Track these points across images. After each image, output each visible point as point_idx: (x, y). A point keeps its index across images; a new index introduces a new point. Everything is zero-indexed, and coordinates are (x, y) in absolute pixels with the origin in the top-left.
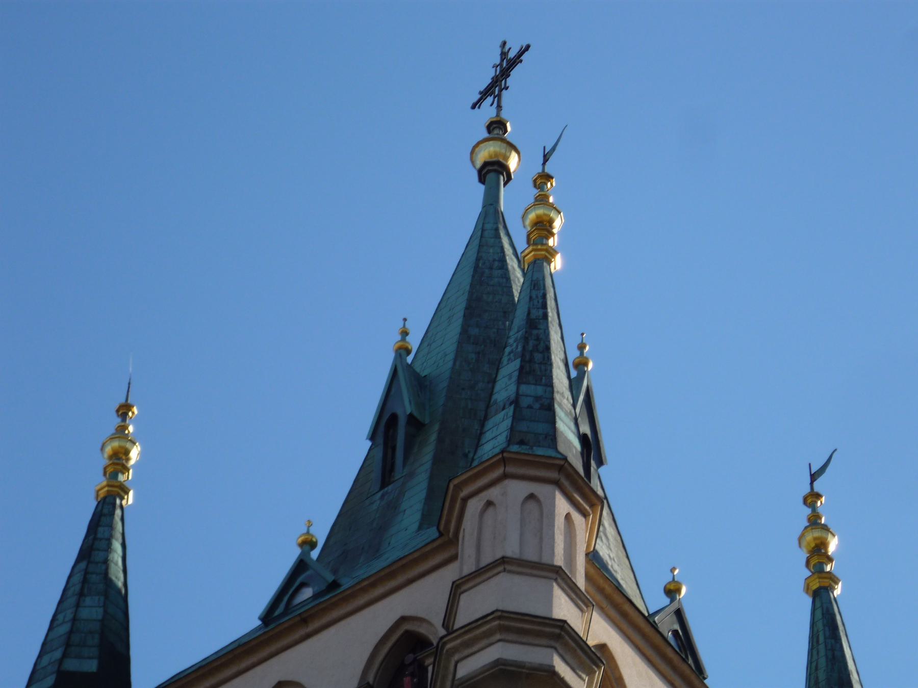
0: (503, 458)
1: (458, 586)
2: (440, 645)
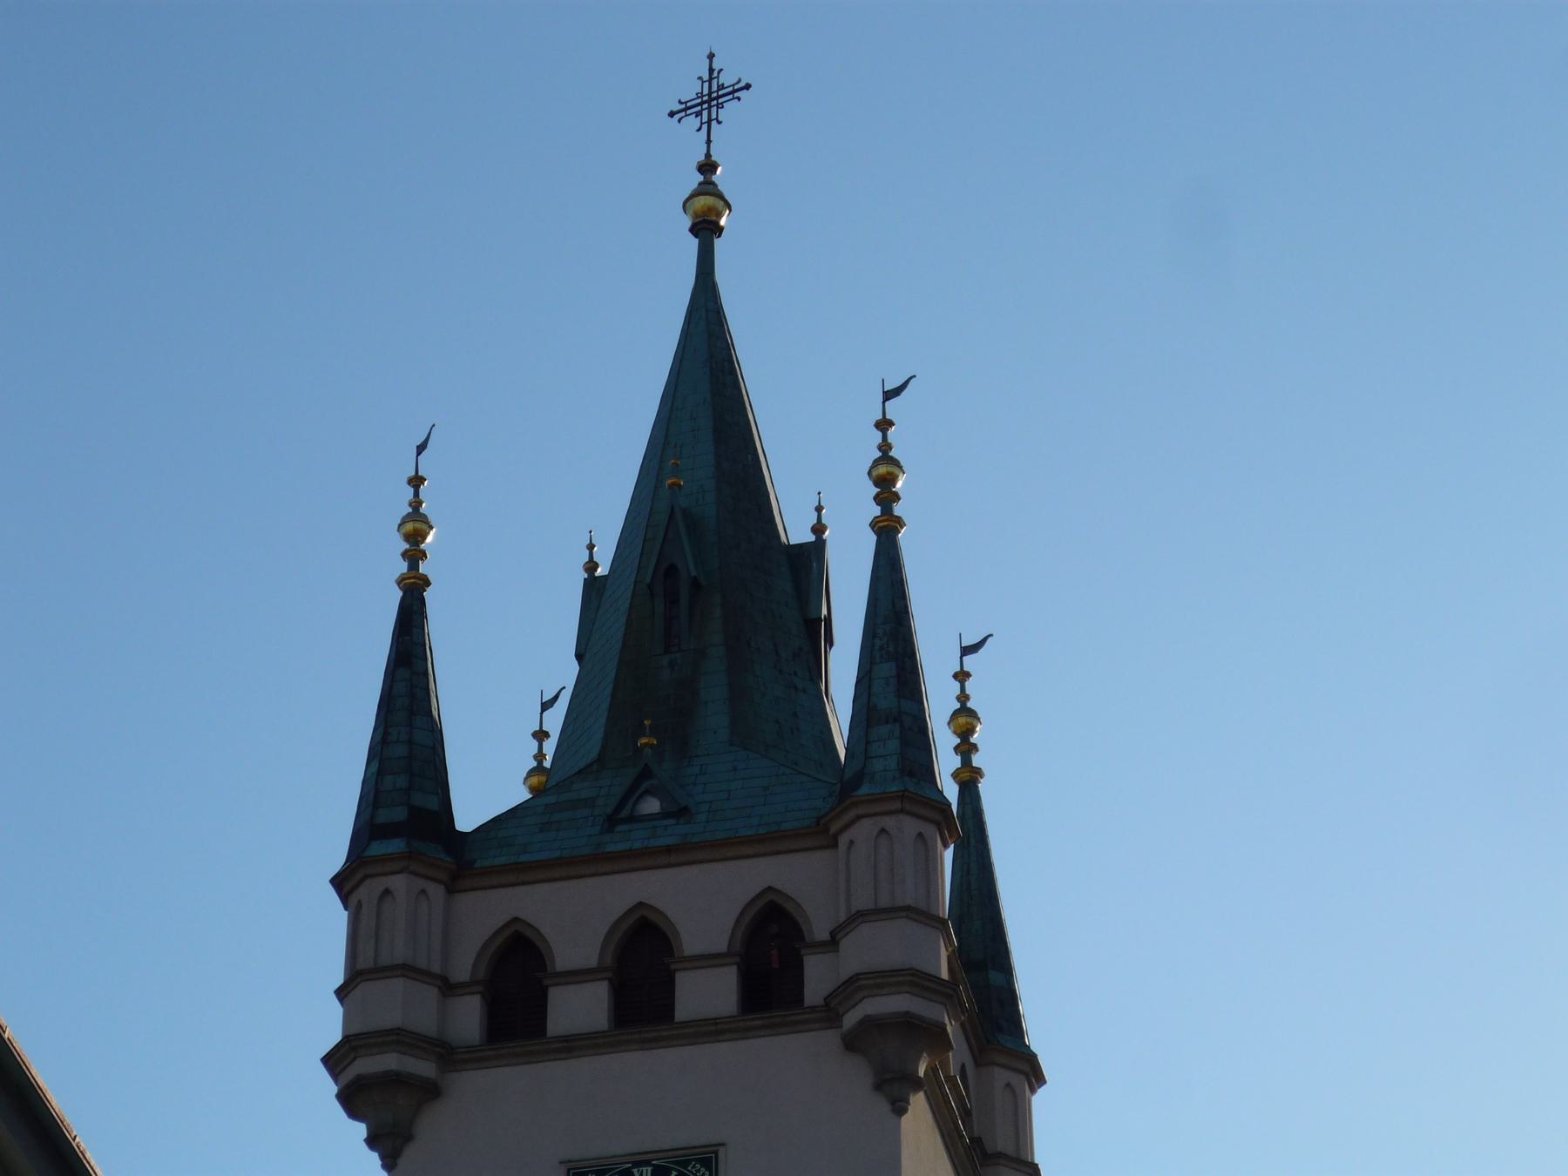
0: (903, 796)
1: (861, 915)
2: (854, 978)
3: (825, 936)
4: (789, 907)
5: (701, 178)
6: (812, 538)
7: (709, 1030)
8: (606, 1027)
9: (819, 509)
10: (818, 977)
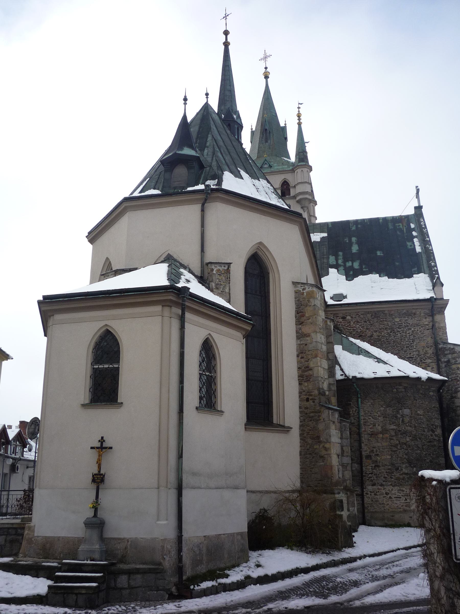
3: (294, 186)
4: (288, 181)
5: (265, 70)
9: (285, 121)
10: (293, 192)
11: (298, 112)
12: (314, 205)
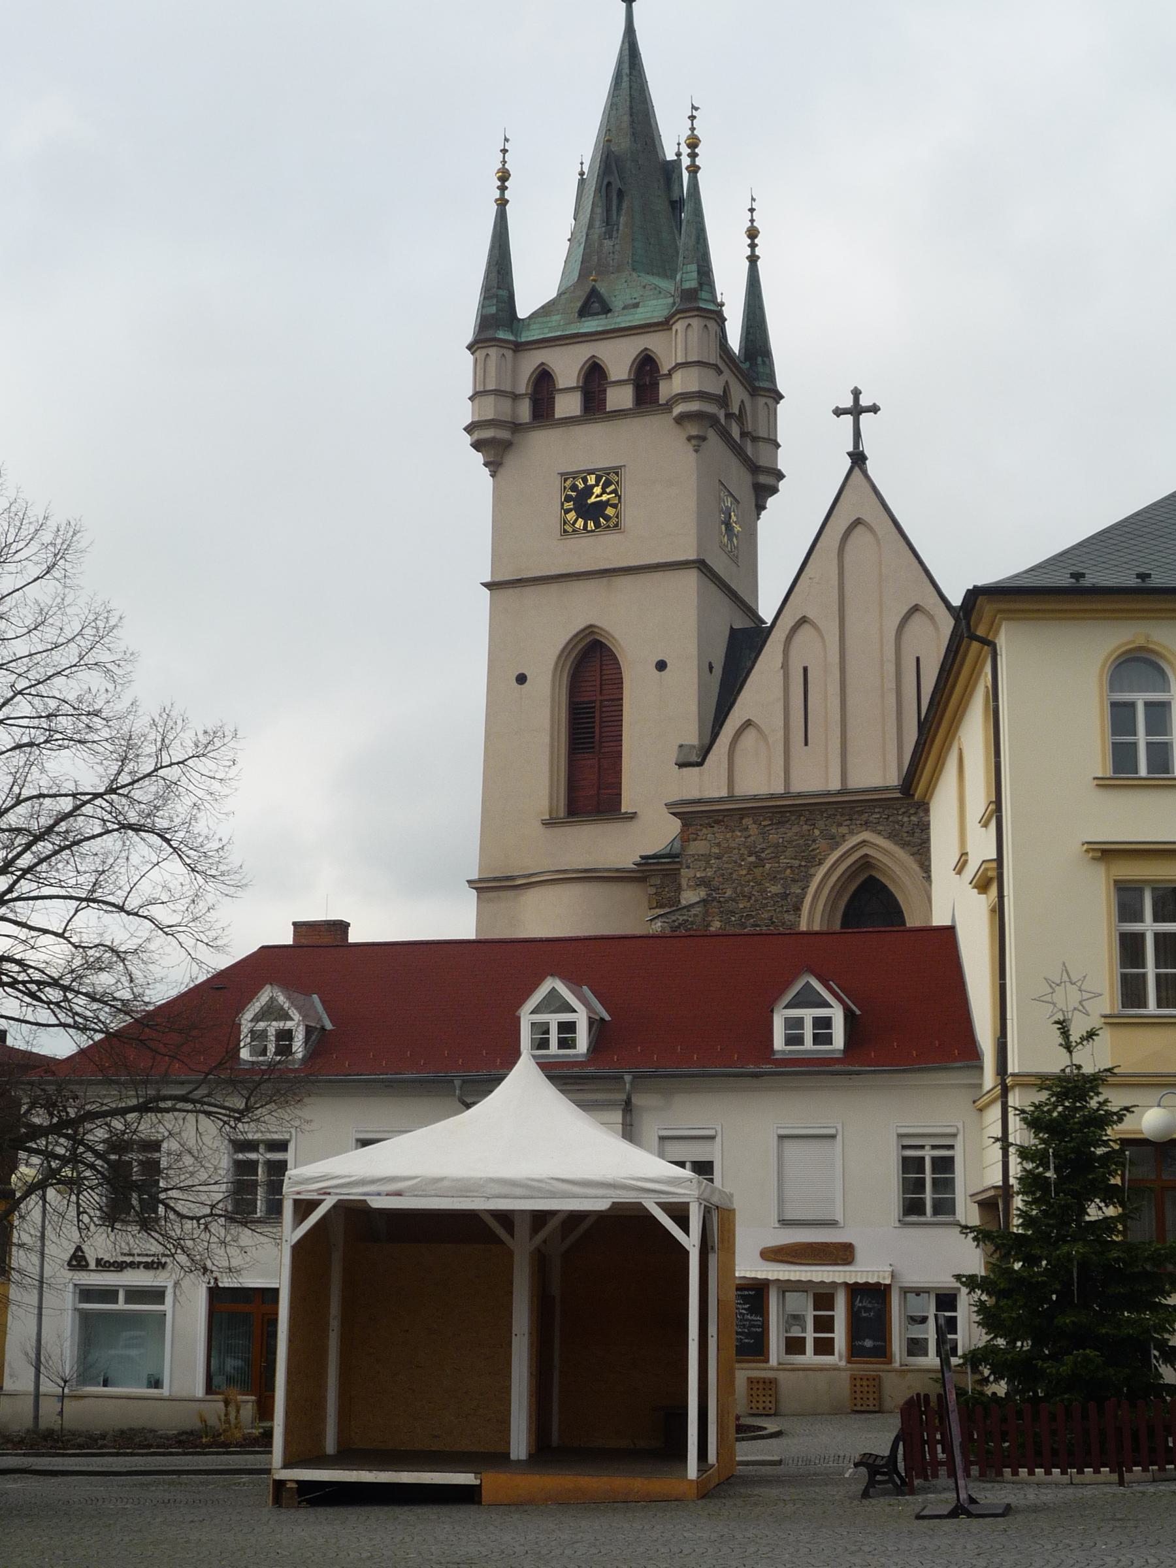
6: (676, 158)
7: (620, 414)
8: (578, 413)
11: (690, 132)
12: (770, 401)
